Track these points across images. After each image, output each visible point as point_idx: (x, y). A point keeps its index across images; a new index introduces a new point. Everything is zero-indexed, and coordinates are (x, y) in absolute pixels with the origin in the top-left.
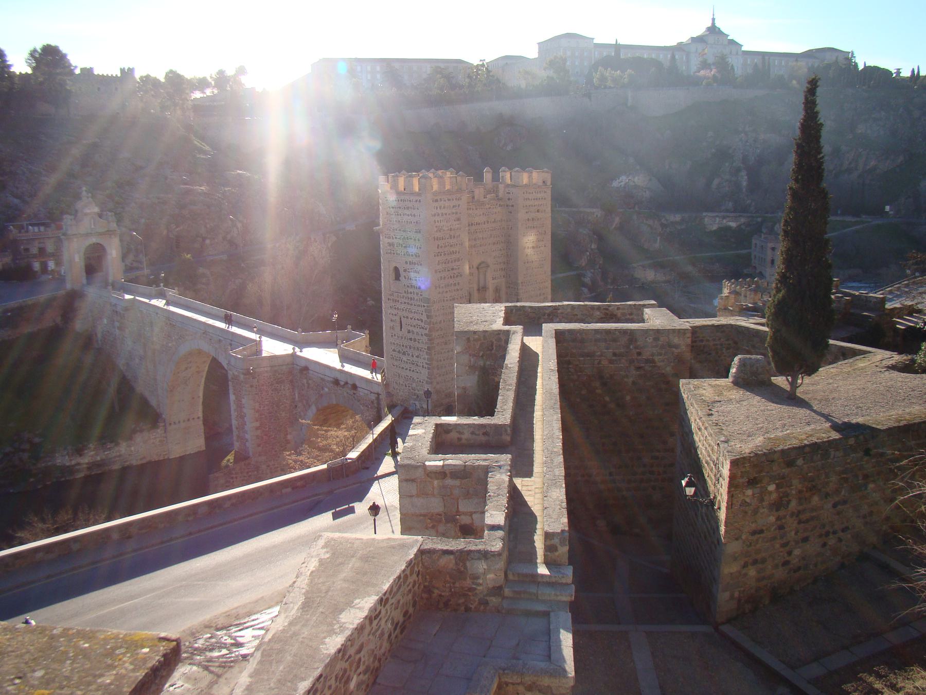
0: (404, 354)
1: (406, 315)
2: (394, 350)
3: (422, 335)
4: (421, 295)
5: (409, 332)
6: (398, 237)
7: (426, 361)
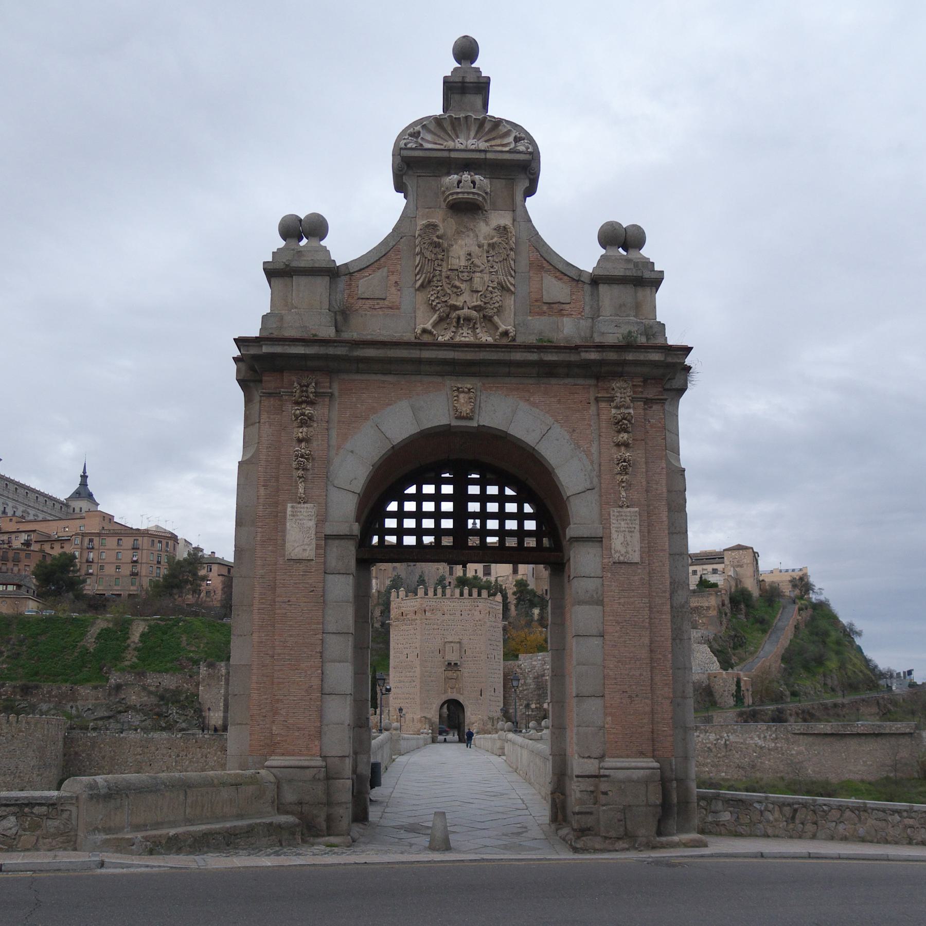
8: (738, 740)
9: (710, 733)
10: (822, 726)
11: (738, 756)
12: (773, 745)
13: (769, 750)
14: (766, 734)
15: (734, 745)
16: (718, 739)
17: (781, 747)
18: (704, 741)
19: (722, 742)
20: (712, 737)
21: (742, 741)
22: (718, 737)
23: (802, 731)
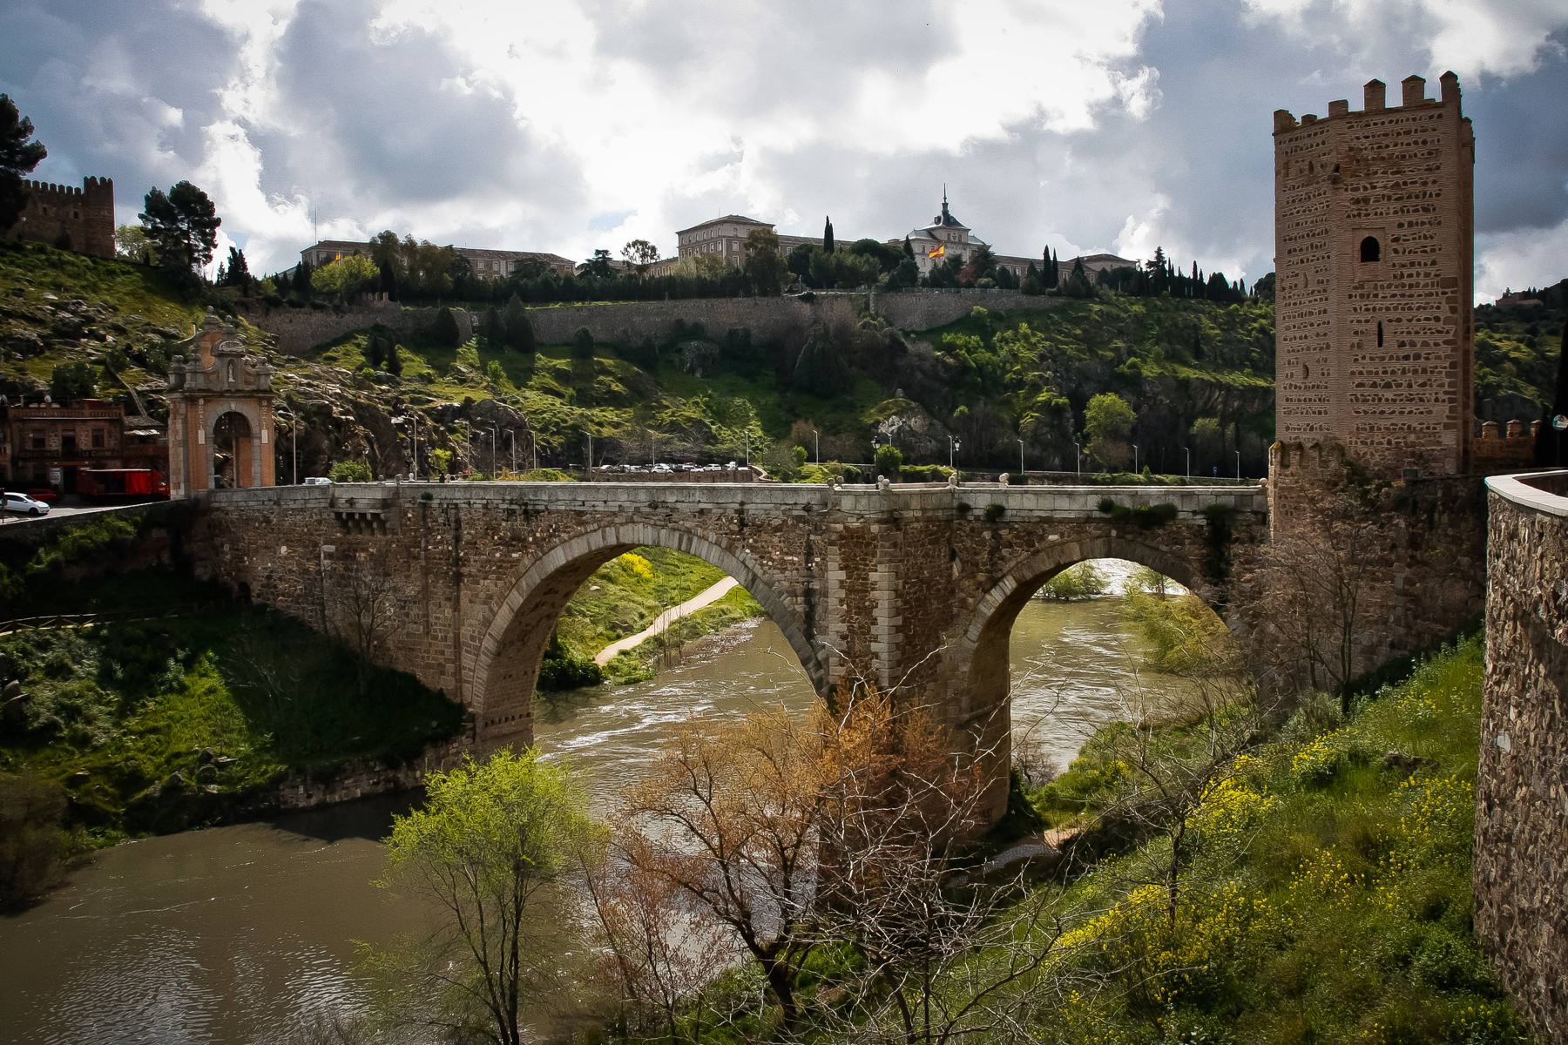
0: (1388, 386)
1: (1393, 315)
2: (1360, 385)
3: (1436, 344)
4: (1436, 276)
5: (1402, 344)
6: (1380, 185)
7: (1446, 388)
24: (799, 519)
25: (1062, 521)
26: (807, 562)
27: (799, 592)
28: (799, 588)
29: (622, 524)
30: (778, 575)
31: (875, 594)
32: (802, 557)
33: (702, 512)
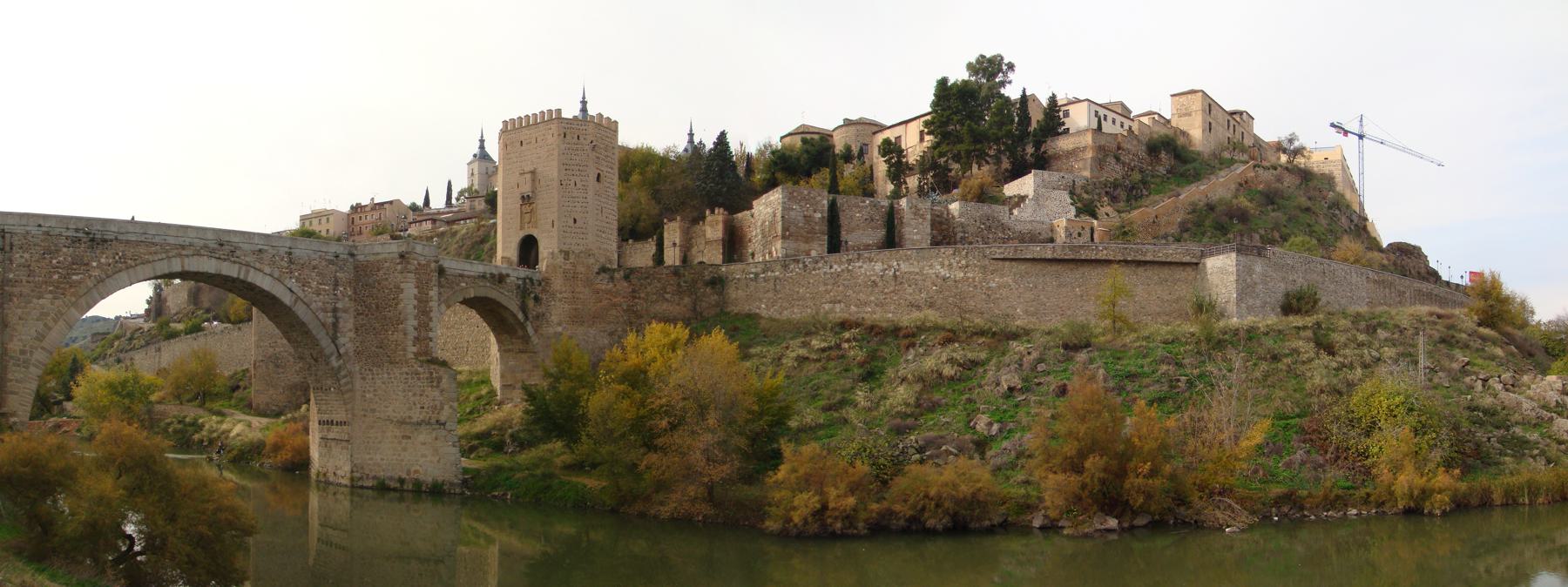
8: (912, 270)
9: (876, 262)
10: (1038, 249)
11: (911, 291)
12: (962, 275)
13: (955, 281)
14: (952, 261)
15: (906, 276)
16: (886, 269)
17: (974, 278)
18: (868, 273)
19: (891, 273)
20: (878, 267)
21: (917, 270)
22: (886, 266)
23: (1006, 255)
24: (331, 262)
25: (469, 277)
26: (334, 290)
27: (329, 309)
28: (329, 307)
29: (187, 256)
30: (315, 297)
31: (431, 304)
32: (332, 287)
33: (260, 250)
